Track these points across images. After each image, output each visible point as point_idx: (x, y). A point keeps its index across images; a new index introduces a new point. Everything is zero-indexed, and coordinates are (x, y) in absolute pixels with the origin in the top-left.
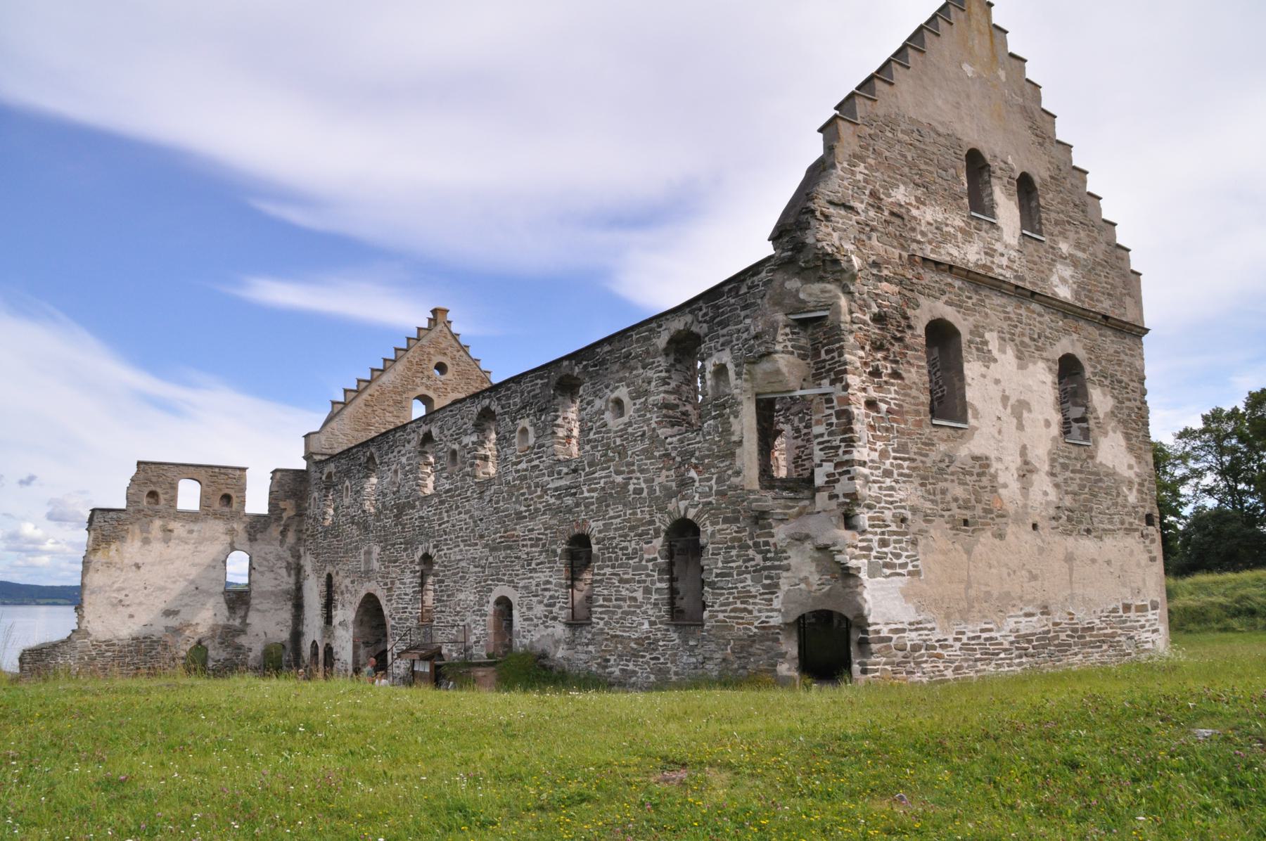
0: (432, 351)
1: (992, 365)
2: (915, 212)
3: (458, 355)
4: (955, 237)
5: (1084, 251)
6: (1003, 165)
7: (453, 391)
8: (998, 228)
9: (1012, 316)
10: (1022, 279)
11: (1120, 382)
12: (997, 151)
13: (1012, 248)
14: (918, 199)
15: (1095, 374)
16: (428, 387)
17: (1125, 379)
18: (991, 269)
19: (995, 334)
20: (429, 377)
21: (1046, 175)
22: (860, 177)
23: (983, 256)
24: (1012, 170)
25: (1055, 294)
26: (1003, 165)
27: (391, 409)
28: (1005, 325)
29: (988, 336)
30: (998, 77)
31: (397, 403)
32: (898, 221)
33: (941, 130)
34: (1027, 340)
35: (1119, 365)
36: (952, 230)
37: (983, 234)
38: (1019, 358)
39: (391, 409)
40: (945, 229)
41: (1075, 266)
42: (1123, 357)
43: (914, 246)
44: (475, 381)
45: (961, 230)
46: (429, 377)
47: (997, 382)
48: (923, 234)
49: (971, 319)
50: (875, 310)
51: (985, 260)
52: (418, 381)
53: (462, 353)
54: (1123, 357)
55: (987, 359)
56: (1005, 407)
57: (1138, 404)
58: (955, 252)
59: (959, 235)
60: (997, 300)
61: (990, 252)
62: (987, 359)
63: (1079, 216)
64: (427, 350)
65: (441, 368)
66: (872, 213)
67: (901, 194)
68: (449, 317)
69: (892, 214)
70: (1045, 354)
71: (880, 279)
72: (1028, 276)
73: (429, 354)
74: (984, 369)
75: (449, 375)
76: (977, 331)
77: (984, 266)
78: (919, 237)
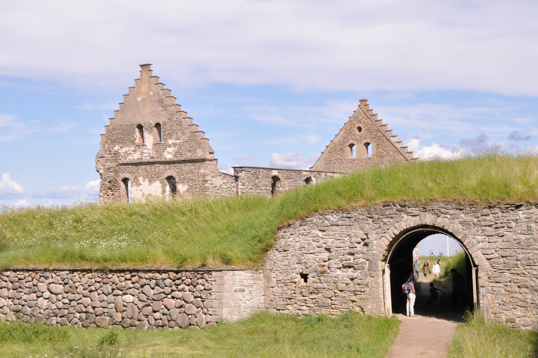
0: (355, 122)
1: (140, 186)
2: (120, 151)
3: (365, 121)
4: (131, 154)
5: (179, 139)
6: (149, 125)
7: (364, 139)
8: (145, 145)
9: (149, 170)
10: (153, 158)
11: (192, 179)
12: (146, 121)
13: (150, 149)
14: (121, 147)
15: (180, 180)
16: (353, 140)
17: (194, 178)
18: (142, 159)
19: (141, 177)
20: (354, 135)
21: (166, 120)
22: (106, 148)
23: (139, 156)
24: (152, 124)
25: (166, 158)
26: (149, 125)
27: (339, 152)
28: (145, 174)
29: (139, 178)
30: (150, 95)
31: (341, 149)
32: (115, 156)
33: (128, 124)
34: (153, 176)
35: (193, 174)
36: (130, 152)
37: (141, 149)
38: (150, 182)
39: (339, 152)
40: (128, 152)
41: (175, 146)
42: (194, 170)
43: (119, 160)
44: (374, 132)
45: (133, 151)
46: (354, 135)
47: (141, 190)
48: (122, 156)
49: (134, 175)
50: (108, 180)
51: (140, 157)
52: (349, 137)
53: (368, 120)
54: (194, 170)
55: (138, 184)
56: (143, 197)
57: (201, 185)
58: (130, 157)
59: (133, 152)
60: (143, 167)
61: (142, 154)
62: (138, 184)
63: (179, 128)
64: (353, 122)
65: (360, 129)
66: (109, 156)
67: (116, 148)
68: (368, 103)
69: (114, 154)
70: (160, 178)
71: (110, 172)
72: (155, 156)
73: (354, 124)
74: (137, 188)
75: (362, 132)
76: (136, 178)
77: (140, 159)
78: (120, 158)
